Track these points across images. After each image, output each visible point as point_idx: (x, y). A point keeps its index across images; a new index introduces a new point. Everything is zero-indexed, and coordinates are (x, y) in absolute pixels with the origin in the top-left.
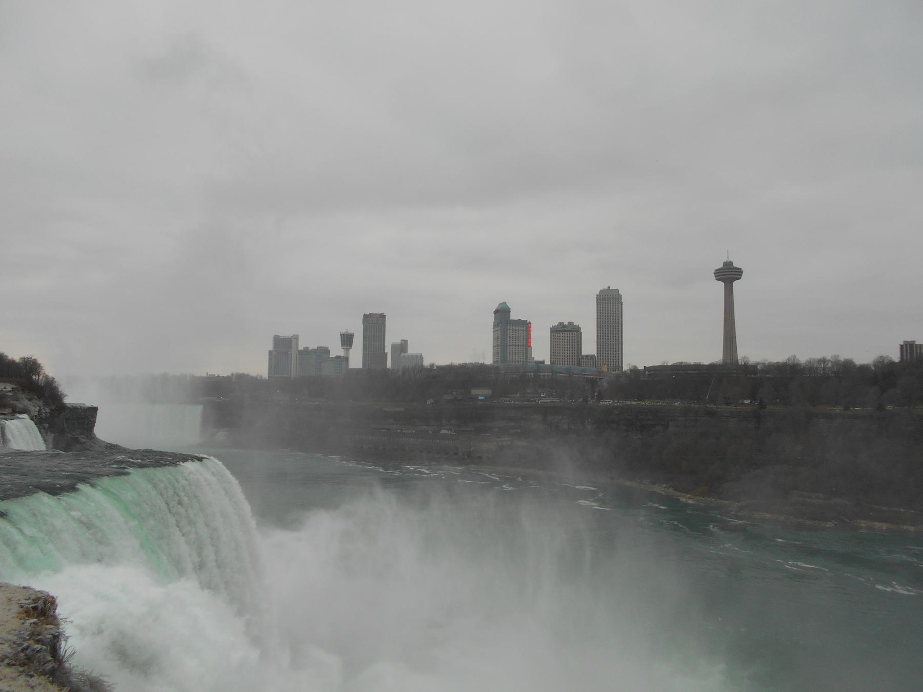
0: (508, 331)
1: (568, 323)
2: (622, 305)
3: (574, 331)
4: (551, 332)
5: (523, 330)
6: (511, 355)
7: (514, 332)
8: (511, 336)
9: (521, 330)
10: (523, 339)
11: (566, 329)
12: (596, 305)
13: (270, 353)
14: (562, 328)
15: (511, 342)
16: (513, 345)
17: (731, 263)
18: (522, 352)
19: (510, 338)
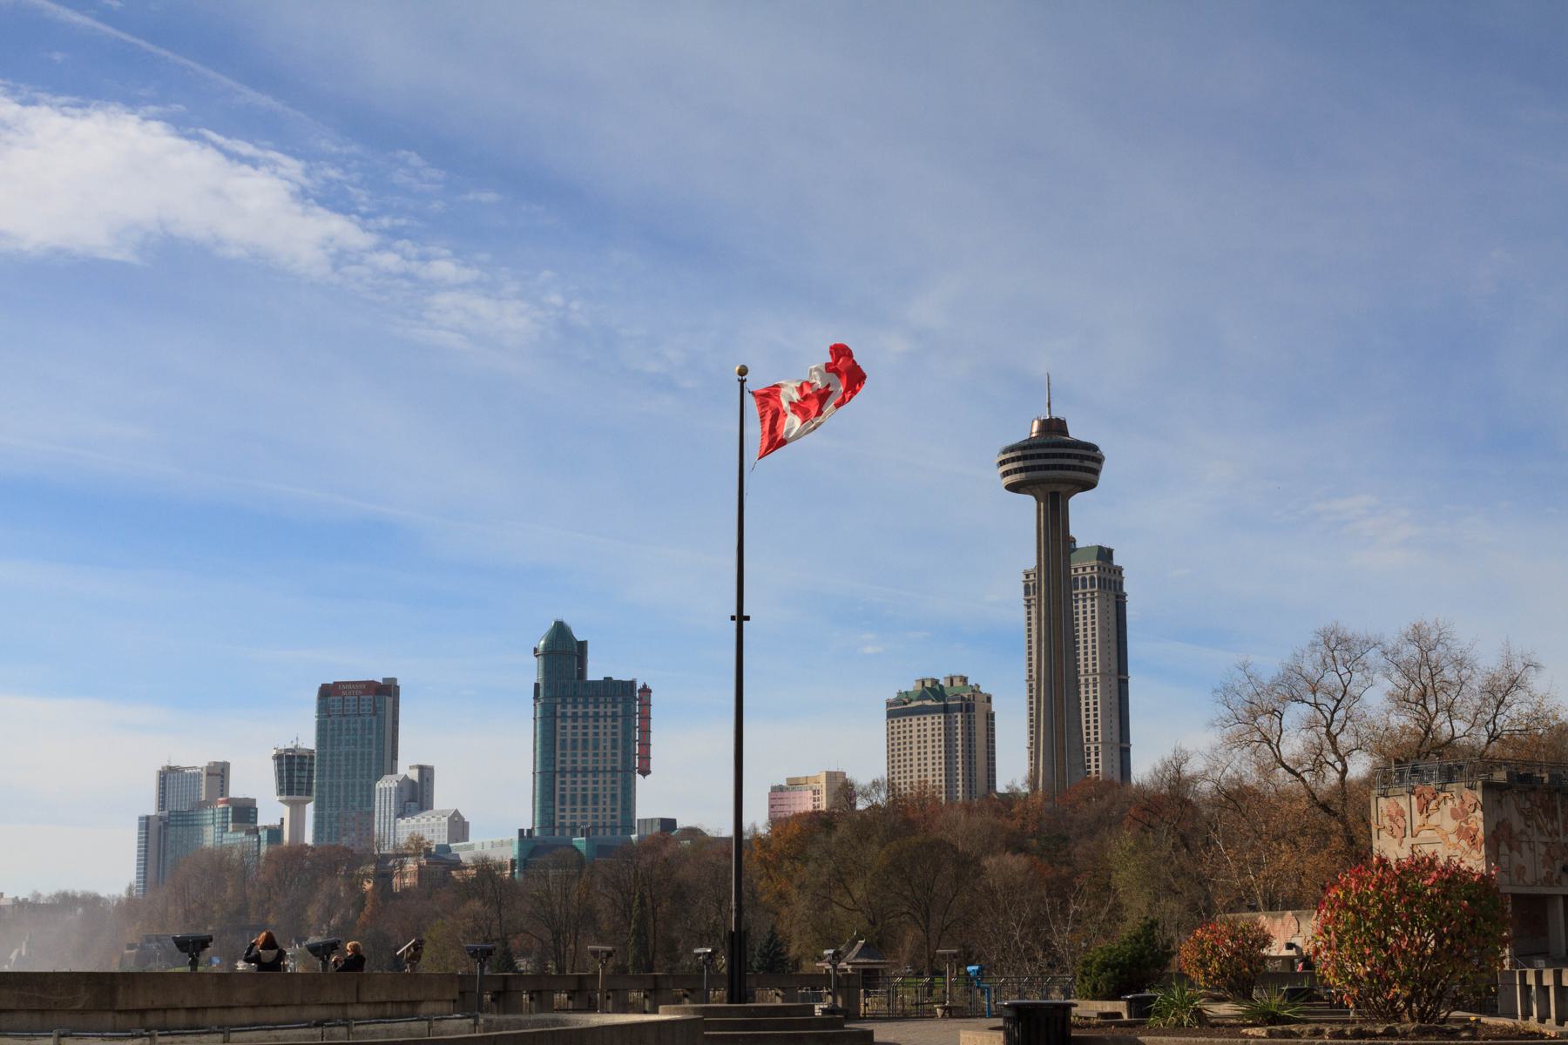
0: (559, 723)
4: (891, 715)
5: (614, 716)
6: (568, 807)
8: (569, 738)
9: (605, 716)
10: (614, 747)
11: (929, 703)
12: (1024, 610)
13: (146, 822)
14: (918, 700)
15: (569, 759)
16: (574, 772)
17: (1054, 427)
18: (608, 793)
19: (563, 747)
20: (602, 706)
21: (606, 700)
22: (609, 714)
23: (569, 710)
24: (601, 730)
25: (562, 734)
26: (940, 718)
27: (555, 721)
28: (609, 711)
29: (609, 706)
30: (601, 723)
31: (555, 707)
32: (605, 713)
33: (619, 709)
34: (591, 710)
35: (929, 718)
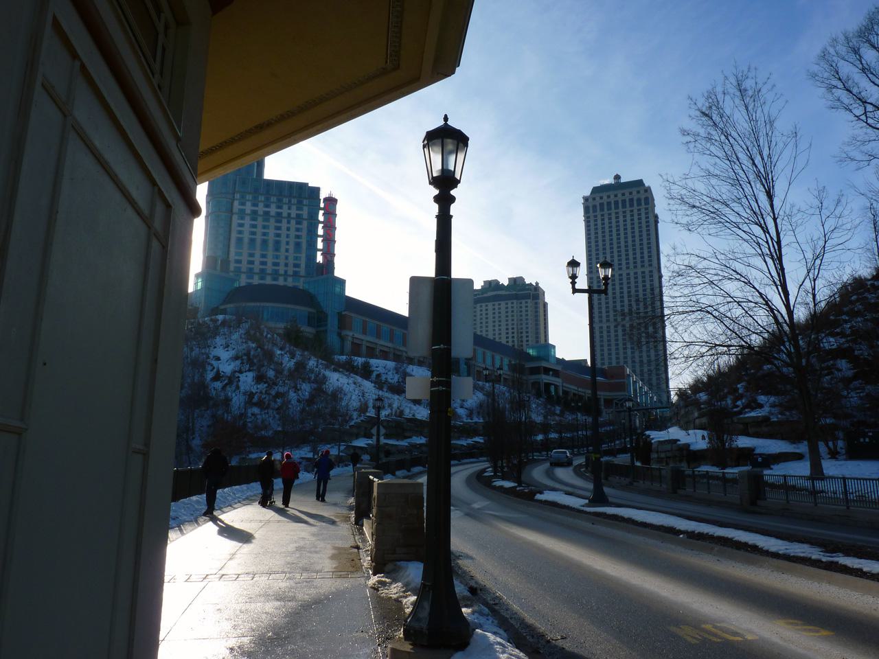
1: (509, 279)
2: (656, 222)
3: (527, 297)
5: (299, 219)
7: (260, 222)
20: (285, 207)
21: (290, 201)
22: (293, 215)
23: (248, 208)
24: (284, 232)
25: (240, 232)
26: (512, 303)
27: (231, 218)
28: (294, 212)
29: (294, 207)
30: (284, 225)
31: (232, 204)
32: (289, 214)
33: (305, 213)
34: (273, 210)
35: (503, 303)
